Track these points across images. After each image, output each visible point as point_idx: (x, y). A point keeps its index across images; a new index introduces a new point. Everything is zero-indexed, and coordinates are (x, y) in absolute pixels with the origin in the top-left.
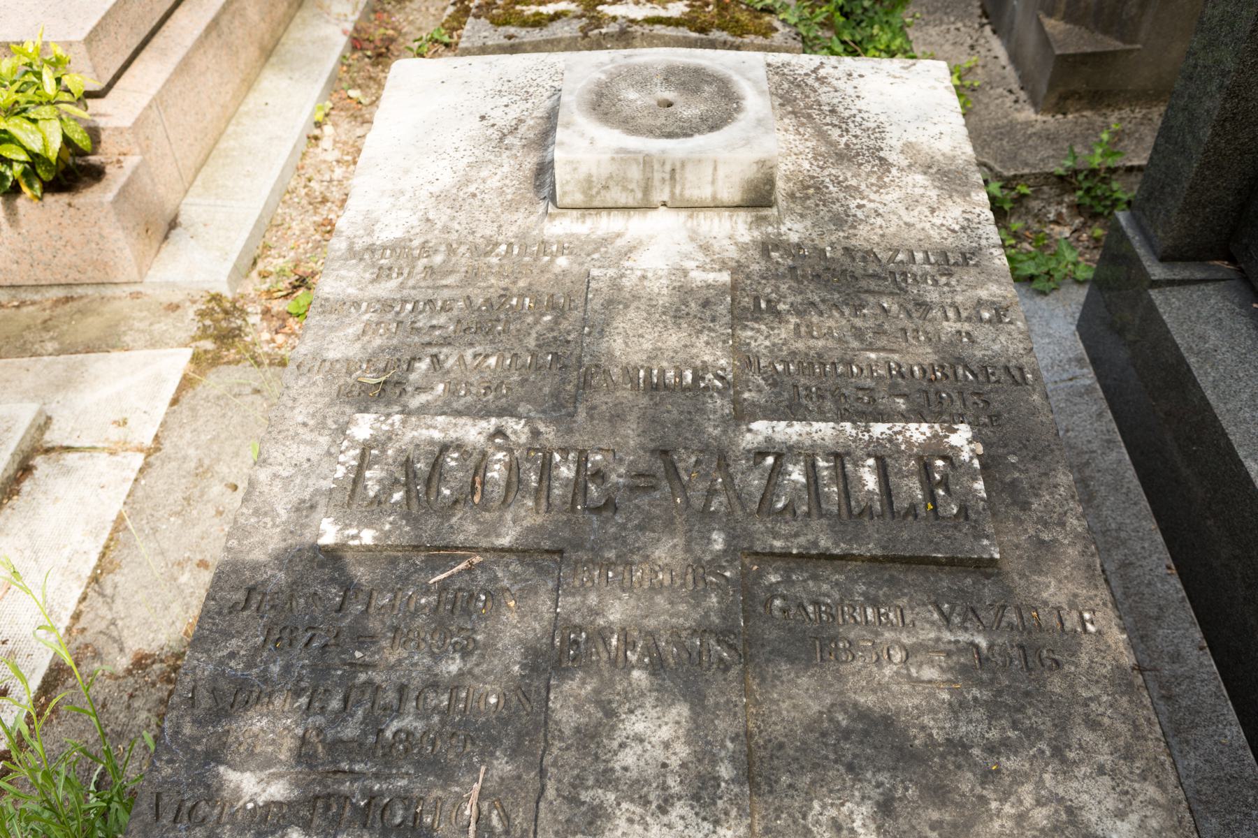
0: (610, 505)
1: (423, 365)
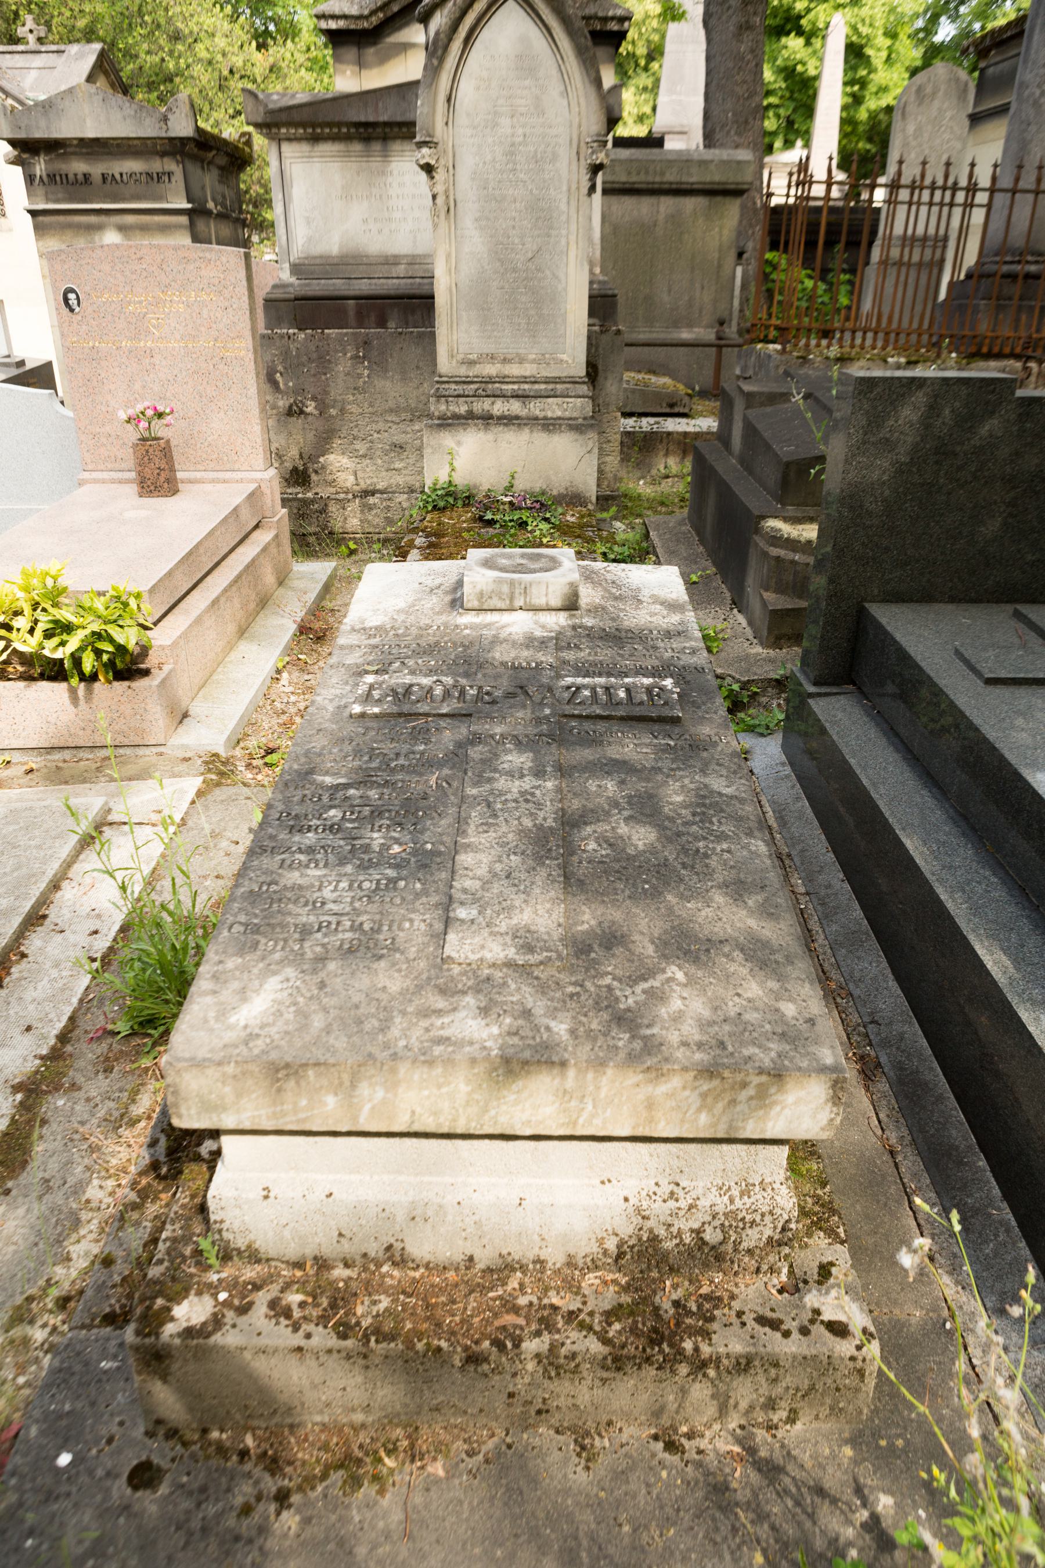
0: (494, 702)
1: (397, 664)
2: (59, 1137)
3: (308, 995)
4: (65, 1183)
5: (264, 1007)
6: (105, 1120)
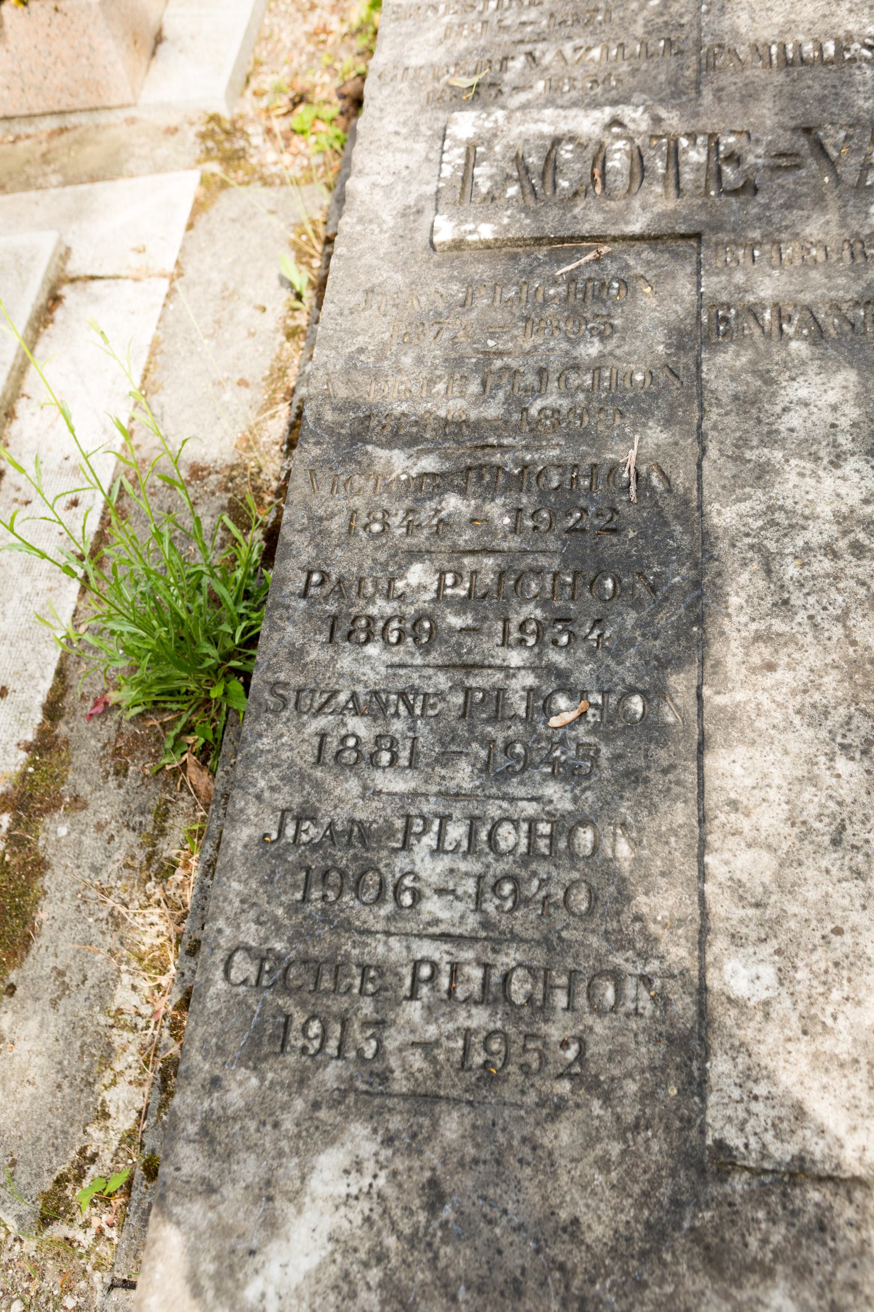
0: (749, 188)
1: (518, 64)
2: (68, 895)
3: (406, 1228)
4: (85, 979)
5: (314, 1260)
6: (127, 866)
